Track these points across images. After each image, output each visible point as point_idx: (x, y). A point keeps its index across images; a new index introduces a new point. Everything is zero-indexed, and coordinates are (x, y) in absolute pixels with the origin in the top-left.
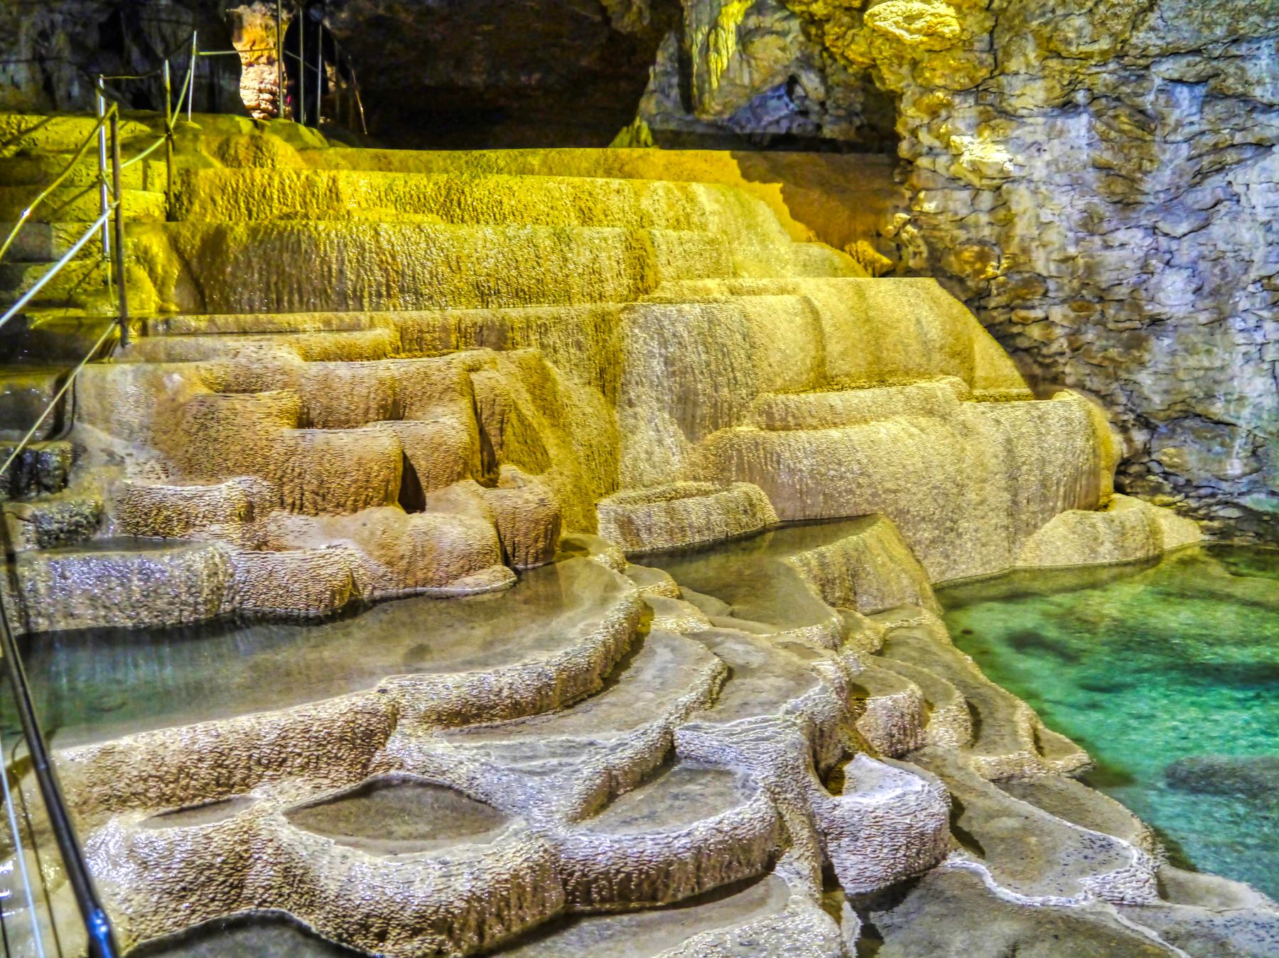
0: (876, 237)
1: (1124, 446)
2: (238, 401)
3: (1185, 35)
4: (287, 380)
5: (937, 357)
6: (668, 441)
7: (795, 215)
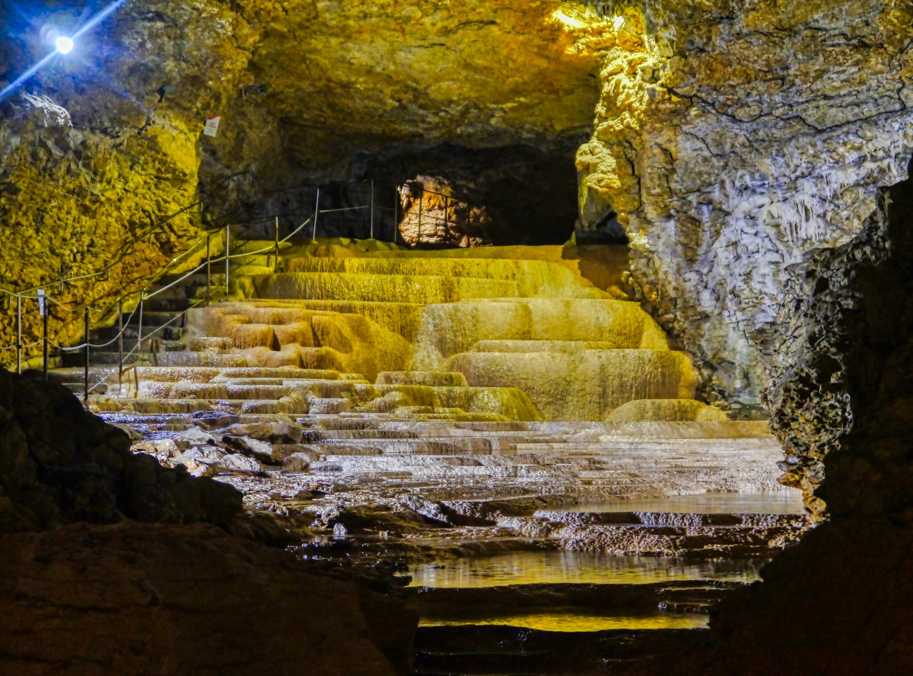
0: (623, 286)
1: (700, 378)
2: (229, 318)
3: (688, 183)
4: (246, 312)
5: (606, 335)
6: (433, 357)
7: (583, 275)
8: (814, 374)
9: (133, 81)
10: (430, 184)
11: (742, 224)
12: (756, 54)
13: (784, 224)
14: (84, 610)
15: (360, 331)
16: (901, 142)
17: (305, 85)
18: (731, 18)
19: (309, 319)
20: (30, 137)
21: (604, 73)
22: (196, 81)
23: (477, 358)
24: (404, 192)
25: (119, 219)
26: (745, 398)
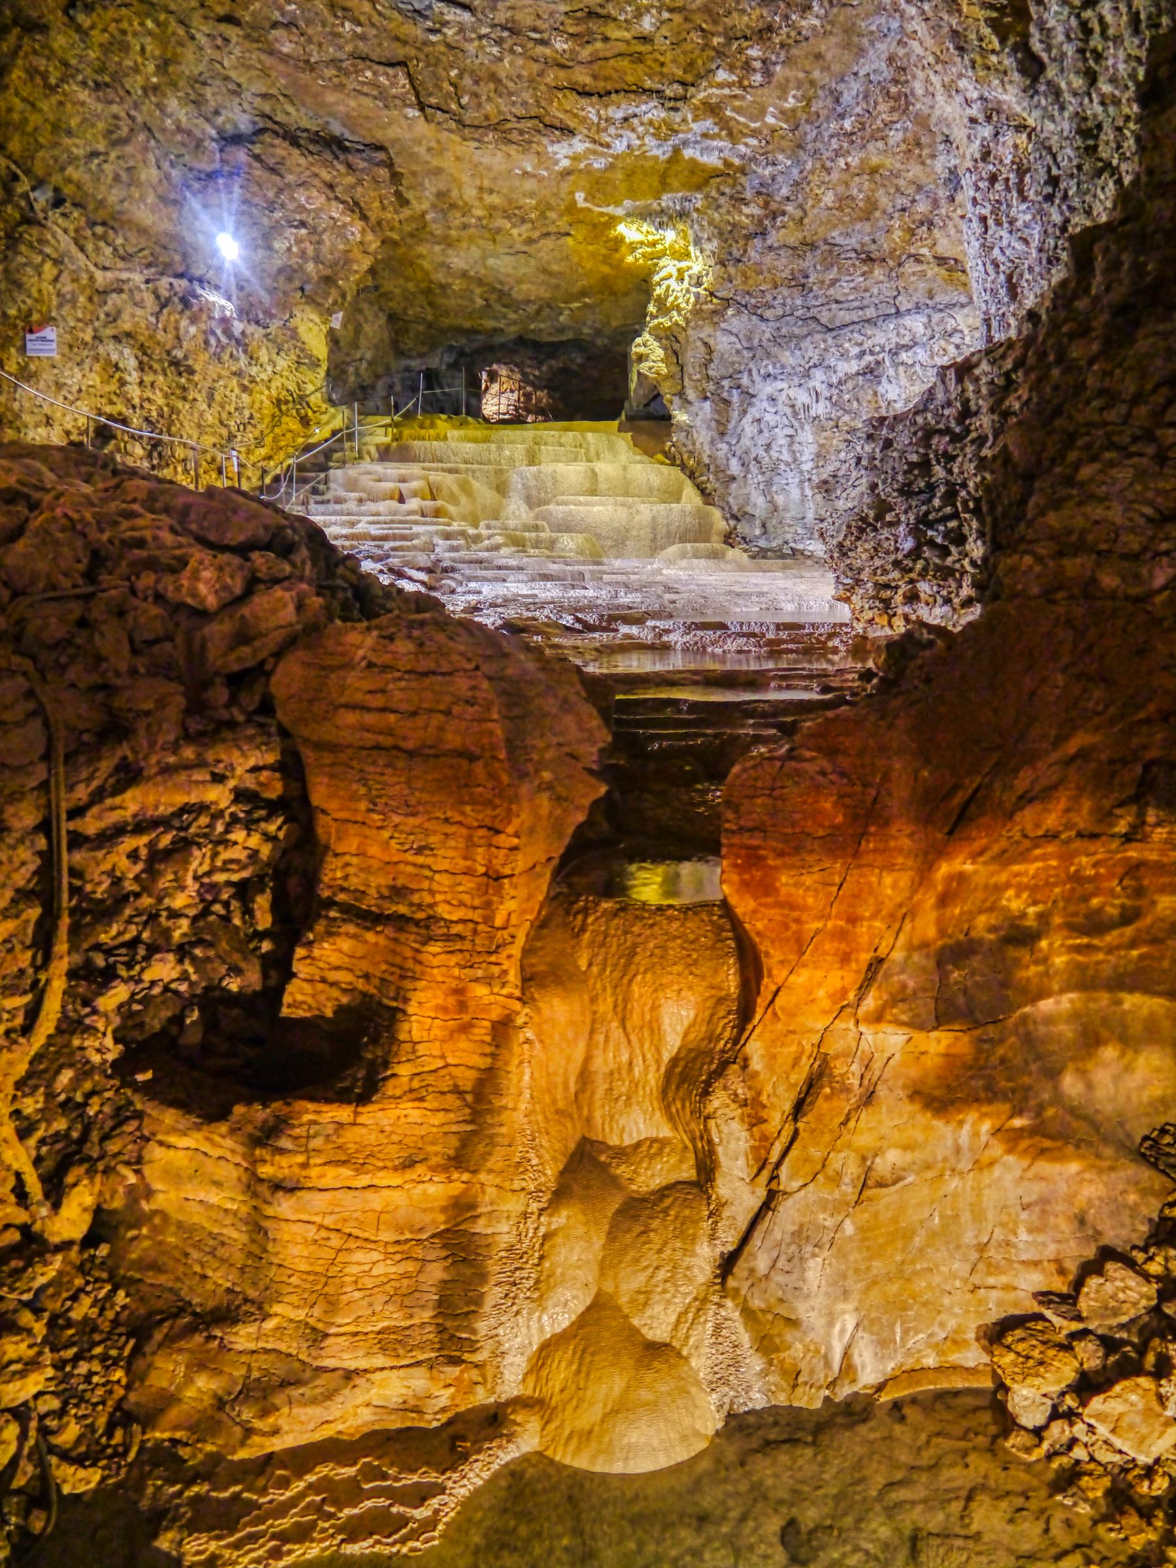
0: (666, 454)
3: (723, 372)
8: (872, 513)
9: (281, 279)
10: (503, 371)
11: (765, 404)
12: (783, 265)
13: (799, 405)
14: (425, 674)
15: (466, 488)
16: (895, 340)
17: (411, 286)
18: (764, 234)
19: (426, 478)
20: (203, 326)
21: (656, 278)
22: (328, 280)
23: (557, 510)
24: (484, 376)
25: (270, 397)
26: (762, 543)
